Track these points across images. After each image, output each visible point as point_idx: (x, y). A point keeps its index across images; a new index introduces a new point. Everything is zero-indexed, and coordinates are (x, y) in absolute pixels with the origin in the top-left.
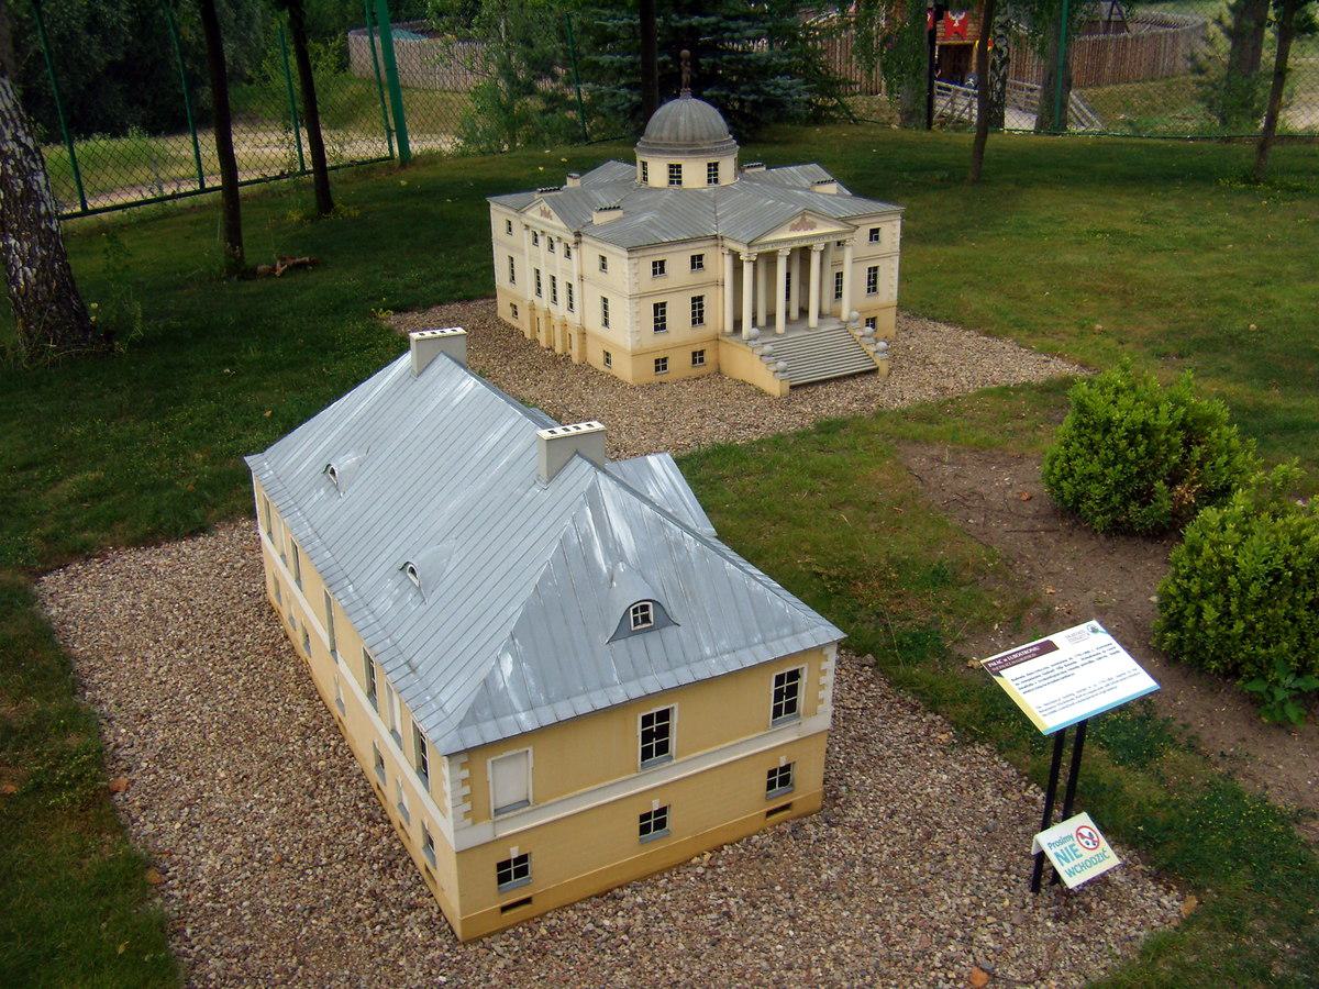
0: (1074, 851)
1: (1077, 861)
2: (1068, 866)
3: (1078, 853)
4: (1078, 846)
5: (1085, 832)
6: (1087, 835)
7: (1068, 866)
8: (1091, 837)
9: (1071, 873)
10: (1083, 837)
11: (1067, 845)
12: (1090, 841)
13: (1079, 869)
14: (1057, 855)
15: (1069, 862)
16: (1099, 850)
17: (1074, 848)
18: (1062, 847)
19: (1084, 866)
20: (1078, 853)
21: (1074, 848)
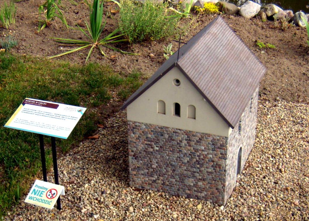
0: (41, 193)
1: (38, 197)
2: (33, 195)
3: (42, 195)
4: (45, 194)
5: (53, 192)
6: (53, 193)
7: (33, 195)
8: (53, 195)
10: (51, 192)
11: (42, 190)
12: (51, 195)
13: (35, 199)
14: (34, 190)
15: (35, 194)
16: (50, 200)
17: (43, 193)
18: (39, 189)
19: (37, 200)
21: (43, 193)
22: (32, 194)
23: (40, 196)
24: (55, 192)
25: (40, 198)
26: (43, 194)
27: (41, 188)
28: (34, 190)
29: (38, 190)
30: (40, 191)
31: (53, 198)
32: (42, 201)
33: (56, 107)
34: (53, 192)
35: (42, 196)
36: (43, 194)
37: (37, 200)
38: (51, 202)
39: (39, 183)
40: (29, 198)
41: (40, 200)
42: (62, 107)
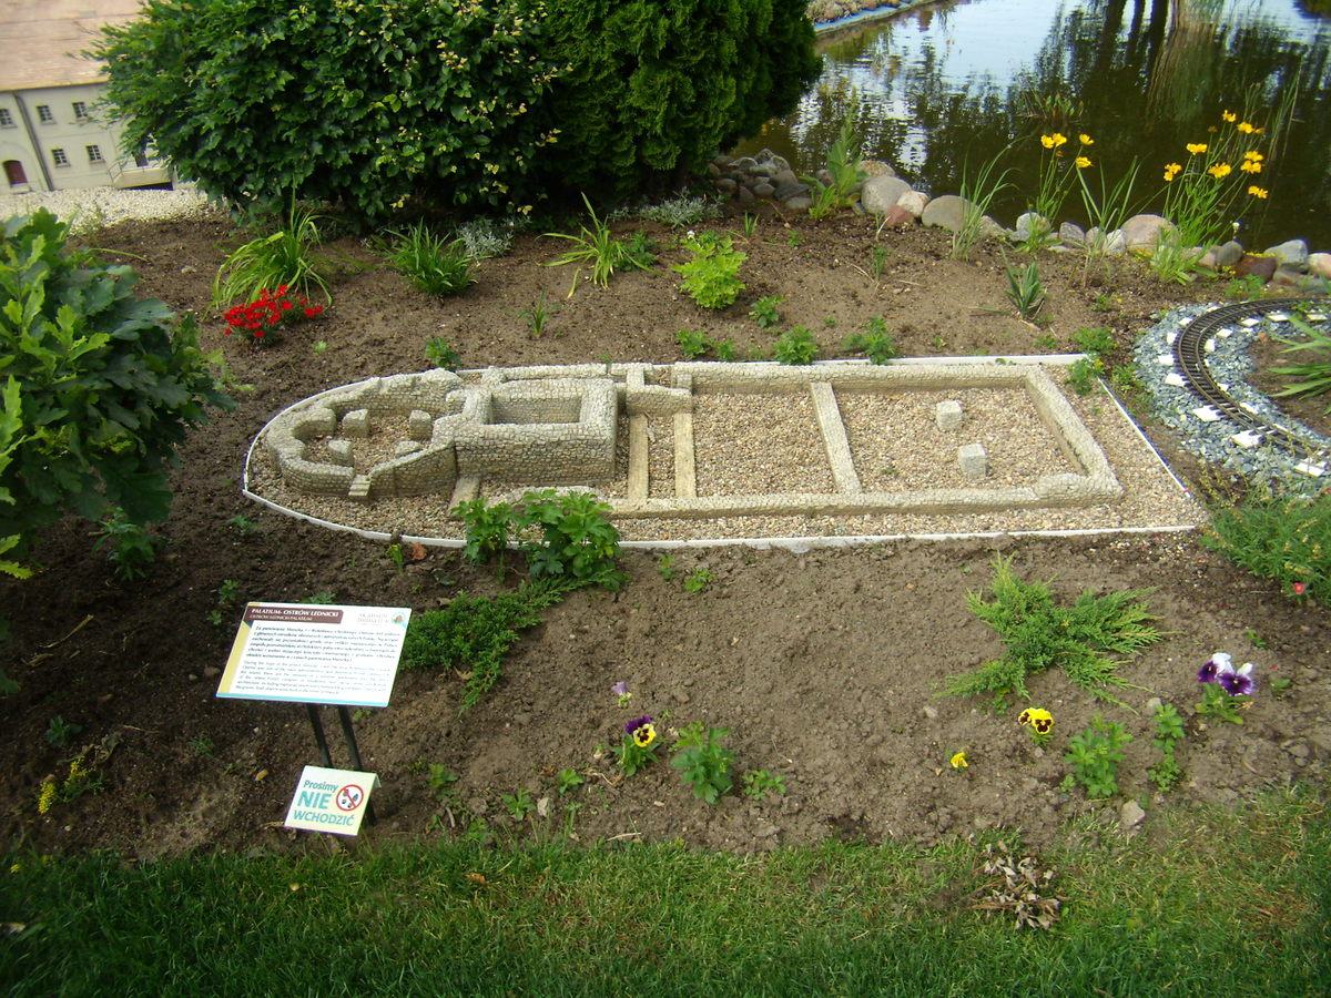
0: (323, 800)
1: (317, 810)
2: (303, 808)
5: (353, 792)
7: (303, 808)
8: (353, 800)
9: (298, 815)
11: (322, 792)
12: (349, 802)
13: (310, 816)
14: (304, 794)
16: (349, 814)
19: (317, 817)
23: (321, 806)
24: (357, 791)
25: (323, 811)
27: (319, 786)
28: (304, 794)
32: (329, 819)
33: (337, 620)
34: (353, 792)
37: (317, 817)
39: (312, 774)
42: (351, 613)
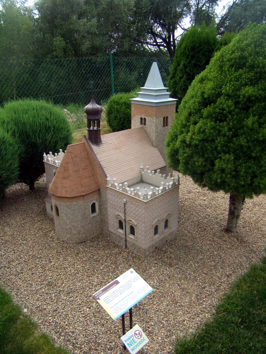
0: (134, 341)
1: (135, 344)
2: (132, 347)
3: (135, 341)
4: (135, 339)
5: (137, 332)
6: (138, 333)
9: (133, 350)
10: (137, 334)
11: (131, 339)
12: (139, 336)
13: (135, 347)
14: (128, 344)
15: (131, 345)
18: (130, 341)
19: (137, 346)
20: (135, 341)
22: (130, 347)
23: (135, 343)
24: (139, 331)
25: (136, 343)
26: (135, 340)
27: (129, 339)
29: (130, 342)
30: (131, 341)
31: (142, 335)
32: (140, 343)
35: (136, 342)
36: (135, 340)
37: (137, 346)
38: (144, 338)
40: (133, 351)
41: (139, 344)
